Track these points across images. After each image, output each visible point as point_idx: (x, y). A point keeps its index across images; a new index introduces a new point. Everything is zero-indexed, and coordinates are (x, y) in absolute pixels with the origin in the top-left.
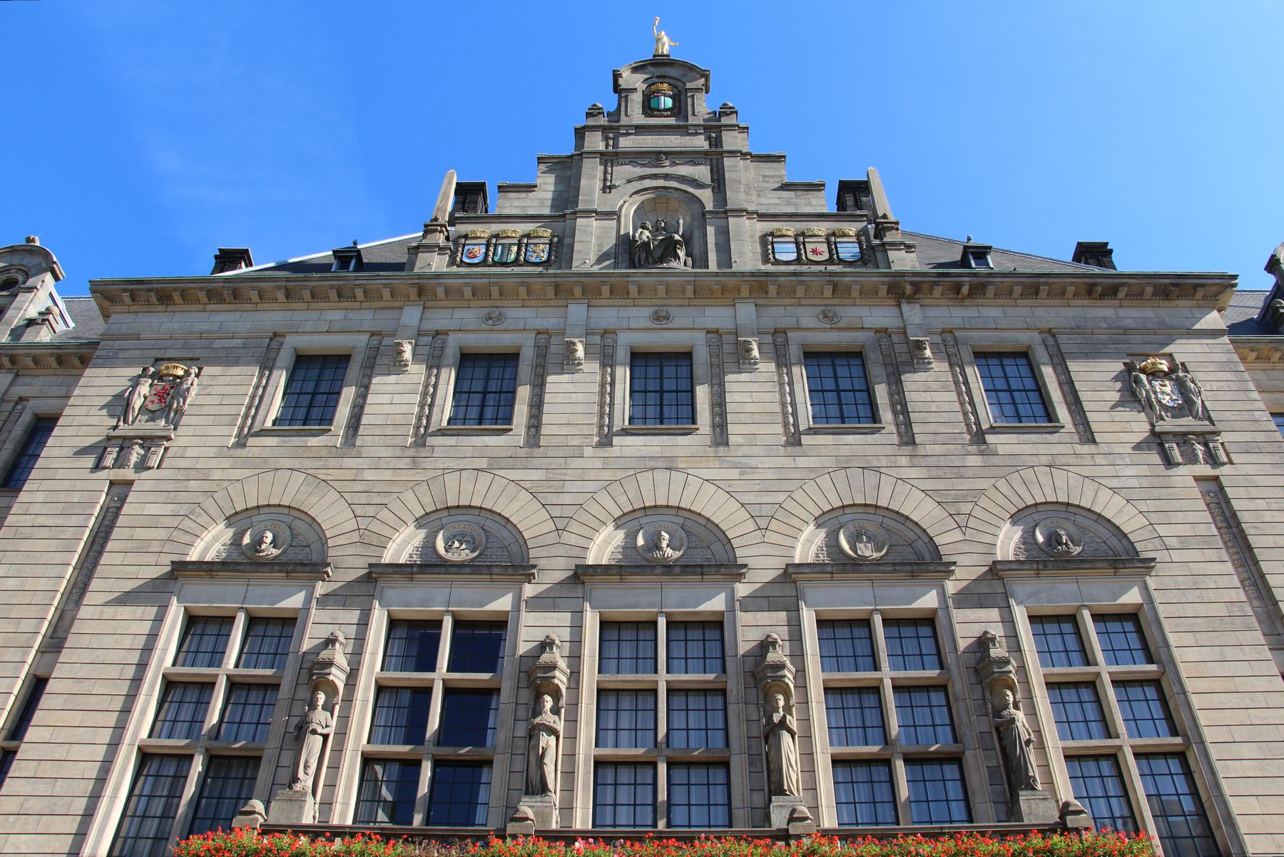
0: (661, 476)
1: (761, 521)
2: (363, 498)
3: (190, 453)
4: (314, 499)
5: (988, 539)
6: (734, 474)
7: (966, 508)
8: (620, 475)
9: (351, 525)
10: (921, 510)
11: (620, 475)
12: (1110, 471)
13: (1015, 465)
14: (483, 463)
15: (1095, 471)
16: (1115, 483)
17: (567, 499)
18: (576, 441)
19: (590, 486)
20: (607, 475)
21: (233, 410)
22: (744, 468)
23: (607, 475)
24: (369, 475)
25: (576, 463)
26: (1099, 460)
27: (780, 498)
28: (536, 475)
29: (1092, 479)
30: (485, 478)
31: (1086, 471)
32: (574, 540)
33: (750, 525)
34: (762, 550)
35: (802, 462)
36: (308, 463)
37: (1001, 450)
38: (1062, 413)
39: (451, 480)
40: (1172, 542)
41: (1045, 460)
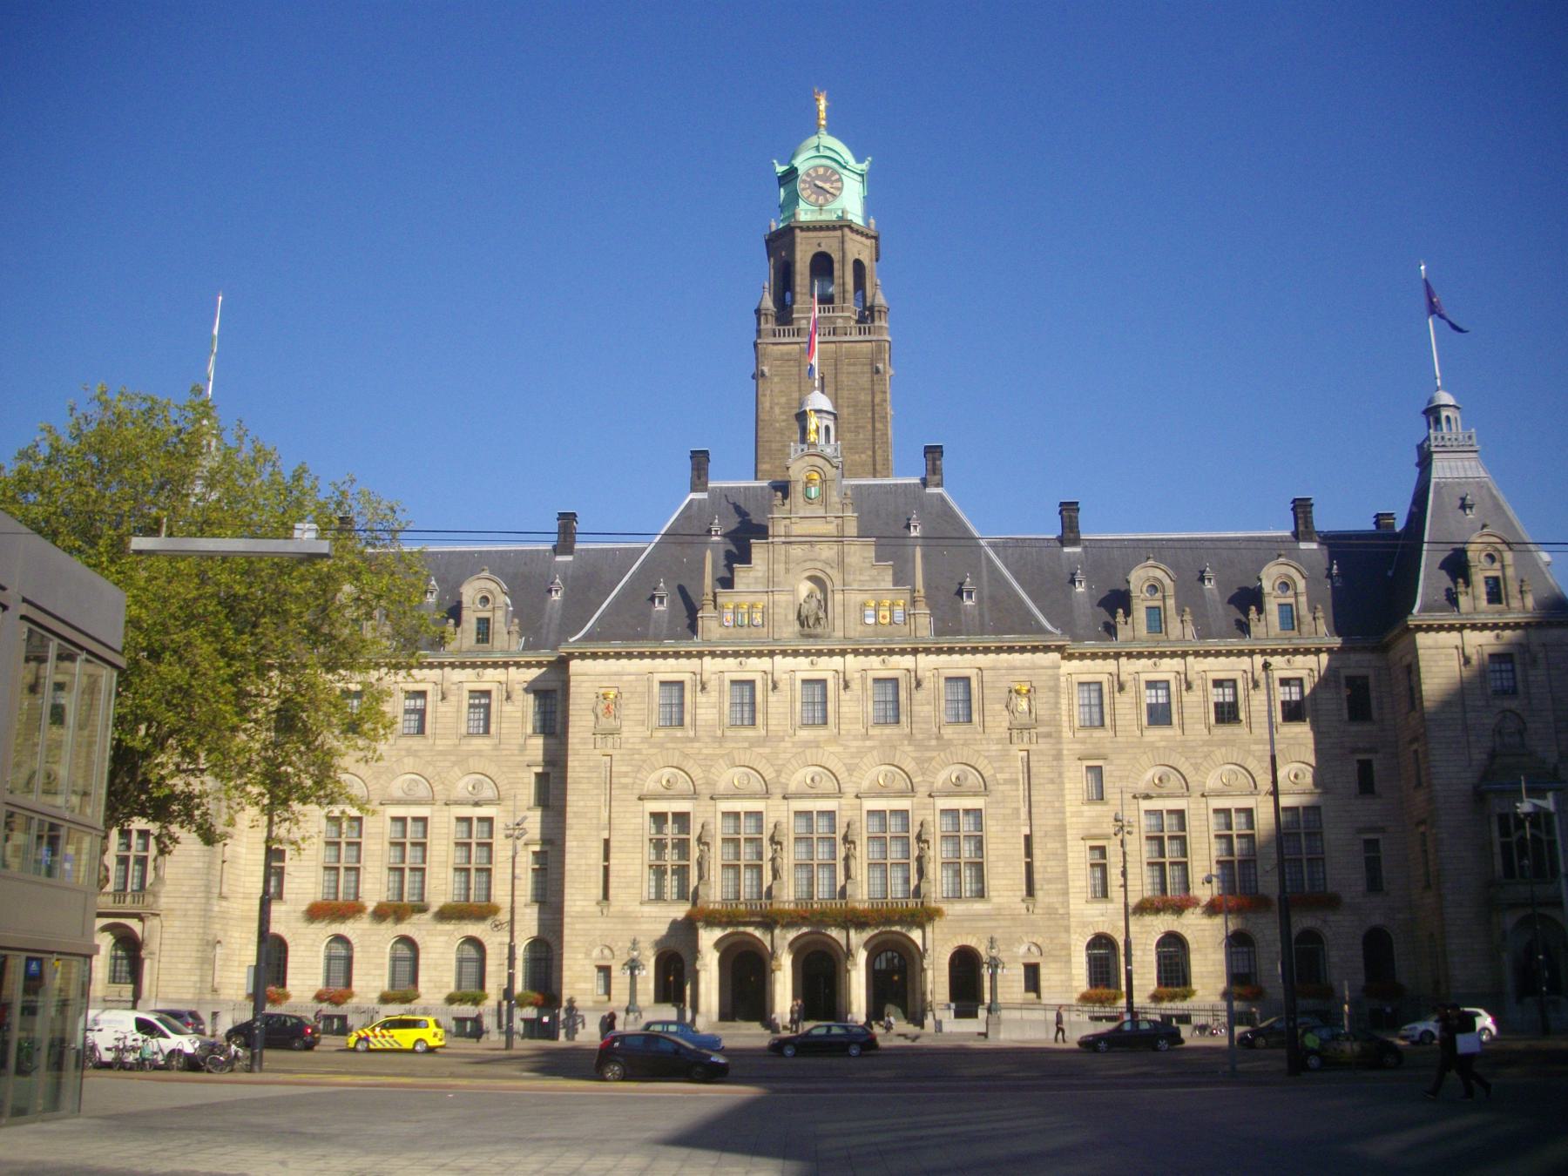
0: (814, 750)
1: (850, 770)
2: (703, 762)
3: (631, 741)
4: (685, 763)
5: (931, 780)
6: (840, 749)
7: (926, 765)
8: (800, 750)
9: (701, 775)
10: (909, 766)
11: (800, 750)
12: (986, 747)
13: (949, 743)
14: (746, 745)
15: (980, 748)
16: (986, 754)
17: (780, 762)
18: (781, 734)
19: (789, 756)
20: (794, 750)
21: (641, 718)
22: (846, 747)
23: (794, 750)
24: (705, 751)
25: (782, 744)
26: (984, 742)
27: (857, 761)
28: (767, 750)
29: (978, 751)
30: (748, 752)
31: (976, 748)
32: (784, 781)
33: (846, 774)
34: (850, 784)
35: (868, 743)
36: (679, 746)
37: (946, 737)
38: (975, 717)
39: (735, 753)
40: (1002, 781)
41: (961, 742)
